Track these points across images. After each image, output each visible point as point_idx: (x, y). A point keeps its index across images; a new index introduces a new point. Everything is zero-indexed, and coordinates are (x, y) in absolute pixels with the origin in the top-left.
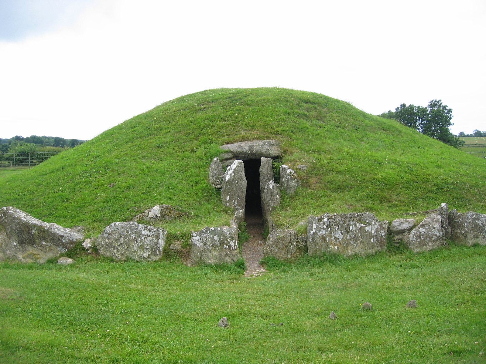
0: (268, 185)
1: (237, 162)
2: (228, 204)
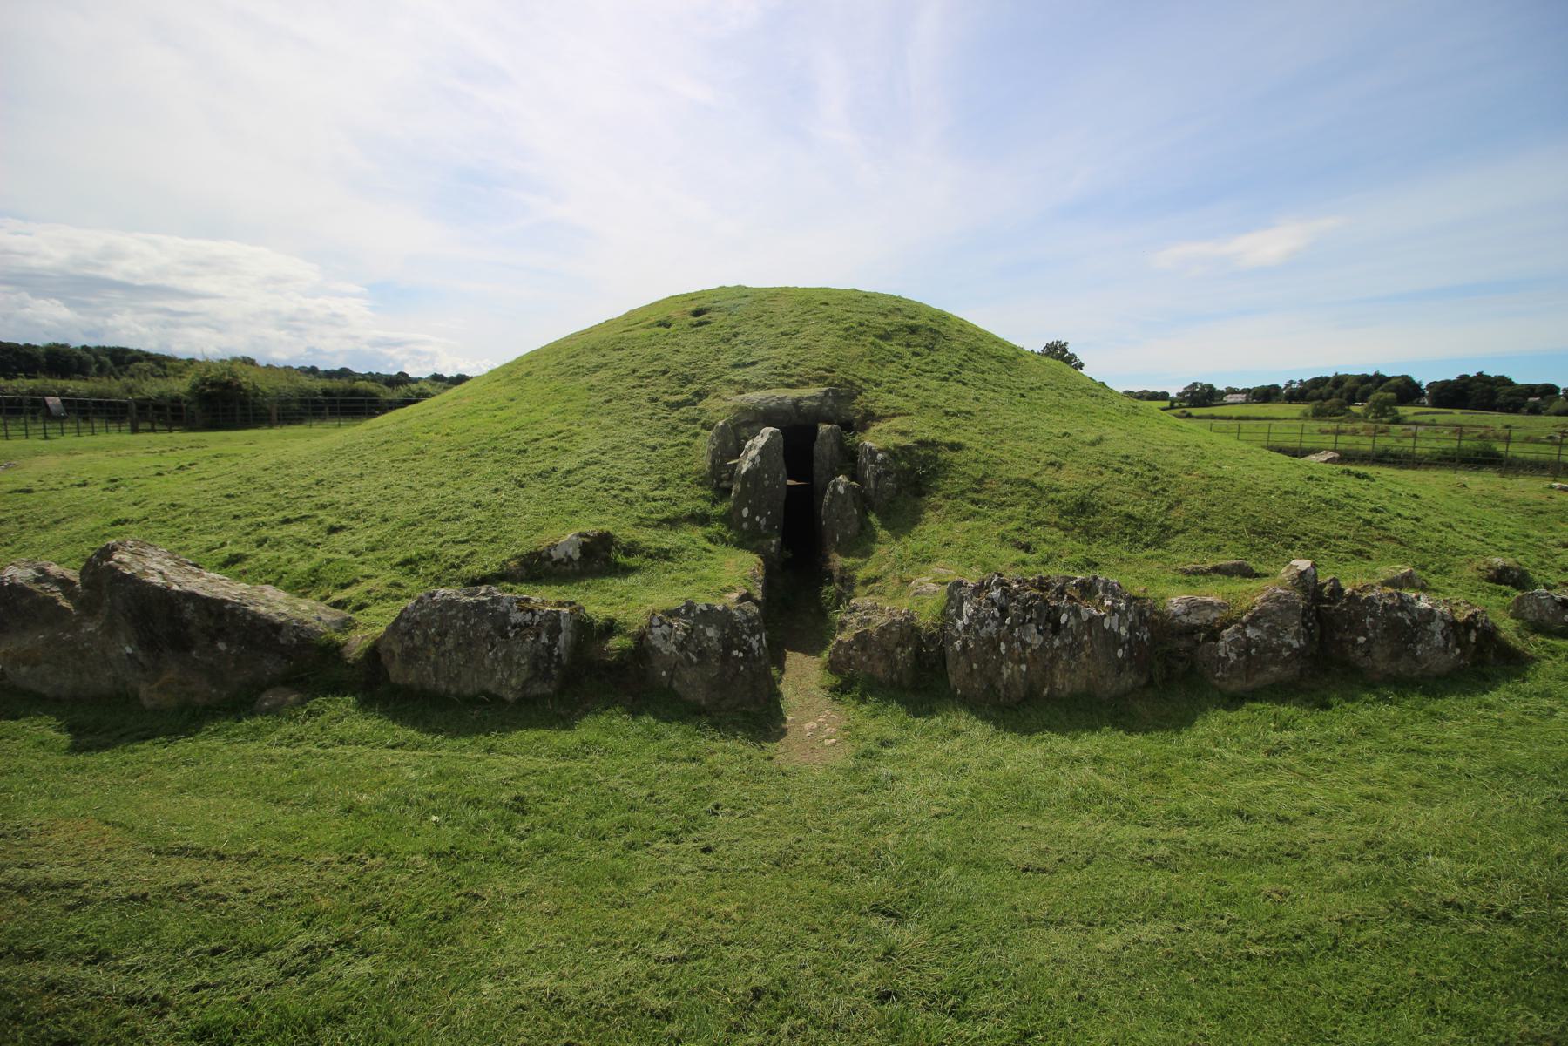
0: (835, 485)
1: (767, 431)
2: (745, 525)
